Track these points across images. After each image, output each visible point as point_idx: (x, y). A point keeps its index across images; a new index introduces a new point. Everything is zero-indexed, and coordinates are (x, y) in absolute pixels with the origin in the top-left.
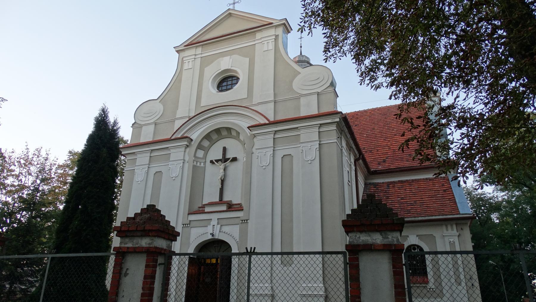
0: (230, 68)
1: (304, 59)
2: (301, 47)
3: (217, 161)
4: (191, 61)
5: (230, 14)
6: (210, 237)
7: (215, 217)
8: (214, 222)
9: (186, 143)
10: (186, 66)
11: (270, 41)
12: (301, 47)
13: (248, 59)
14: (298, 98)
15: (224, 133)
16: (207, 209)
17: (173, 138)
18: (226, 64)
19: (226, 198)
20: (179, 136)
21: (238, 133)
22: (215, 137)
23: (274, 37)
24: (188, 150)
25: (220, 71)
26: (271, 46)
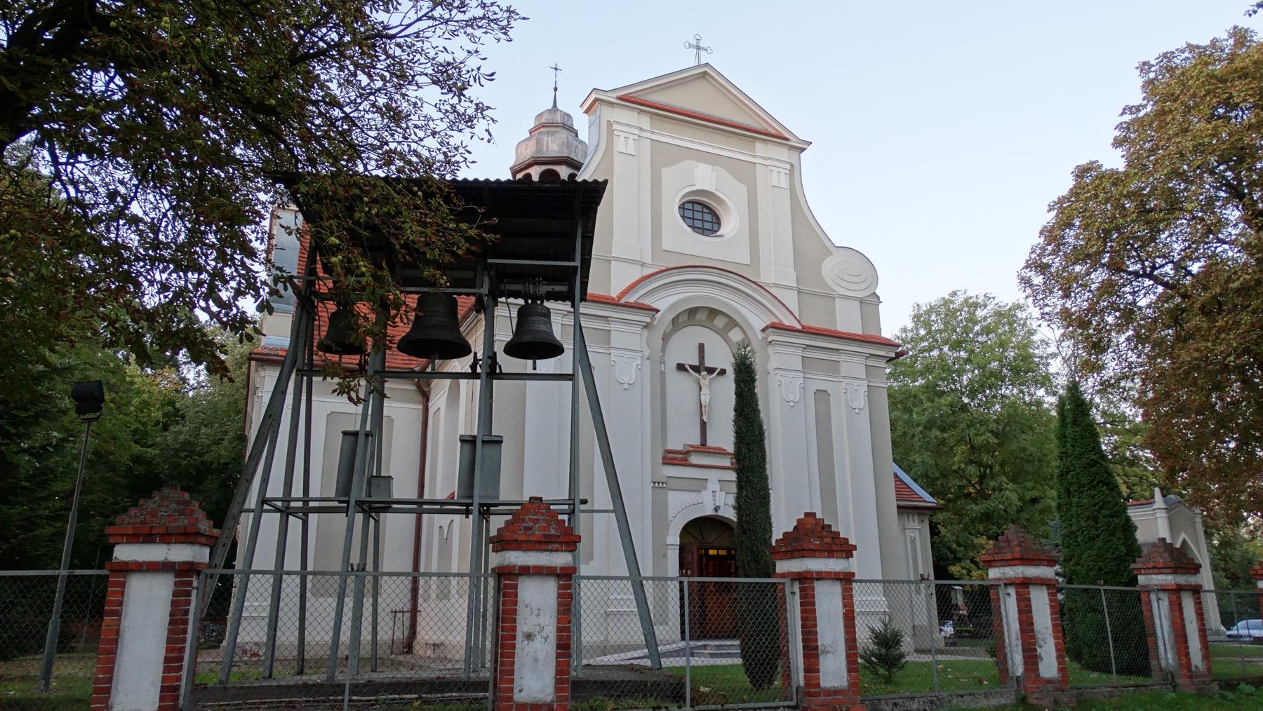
0: (713, 190)
1: (558, 118)
2: (556, 89)
3: (697, 369)
5: (705, 73)
6: (709, 512)
7: (713, 476)
8: (713, 485)
9: (648, 320)
10: (620, 145)
11: (783, 171)
12: (556, 89)
13: (744, 188)
14: (831, 298)
15: (701, 316)
16: (694, 459)
17: (622, 301)
18: (704, 178)
19: (711, 442)
20: (632, 299)
21: (732, 323)
22: (684, 318)
23: (788, 167)
24: (646, 333)
25: (695, 188)
26: (784, 183)
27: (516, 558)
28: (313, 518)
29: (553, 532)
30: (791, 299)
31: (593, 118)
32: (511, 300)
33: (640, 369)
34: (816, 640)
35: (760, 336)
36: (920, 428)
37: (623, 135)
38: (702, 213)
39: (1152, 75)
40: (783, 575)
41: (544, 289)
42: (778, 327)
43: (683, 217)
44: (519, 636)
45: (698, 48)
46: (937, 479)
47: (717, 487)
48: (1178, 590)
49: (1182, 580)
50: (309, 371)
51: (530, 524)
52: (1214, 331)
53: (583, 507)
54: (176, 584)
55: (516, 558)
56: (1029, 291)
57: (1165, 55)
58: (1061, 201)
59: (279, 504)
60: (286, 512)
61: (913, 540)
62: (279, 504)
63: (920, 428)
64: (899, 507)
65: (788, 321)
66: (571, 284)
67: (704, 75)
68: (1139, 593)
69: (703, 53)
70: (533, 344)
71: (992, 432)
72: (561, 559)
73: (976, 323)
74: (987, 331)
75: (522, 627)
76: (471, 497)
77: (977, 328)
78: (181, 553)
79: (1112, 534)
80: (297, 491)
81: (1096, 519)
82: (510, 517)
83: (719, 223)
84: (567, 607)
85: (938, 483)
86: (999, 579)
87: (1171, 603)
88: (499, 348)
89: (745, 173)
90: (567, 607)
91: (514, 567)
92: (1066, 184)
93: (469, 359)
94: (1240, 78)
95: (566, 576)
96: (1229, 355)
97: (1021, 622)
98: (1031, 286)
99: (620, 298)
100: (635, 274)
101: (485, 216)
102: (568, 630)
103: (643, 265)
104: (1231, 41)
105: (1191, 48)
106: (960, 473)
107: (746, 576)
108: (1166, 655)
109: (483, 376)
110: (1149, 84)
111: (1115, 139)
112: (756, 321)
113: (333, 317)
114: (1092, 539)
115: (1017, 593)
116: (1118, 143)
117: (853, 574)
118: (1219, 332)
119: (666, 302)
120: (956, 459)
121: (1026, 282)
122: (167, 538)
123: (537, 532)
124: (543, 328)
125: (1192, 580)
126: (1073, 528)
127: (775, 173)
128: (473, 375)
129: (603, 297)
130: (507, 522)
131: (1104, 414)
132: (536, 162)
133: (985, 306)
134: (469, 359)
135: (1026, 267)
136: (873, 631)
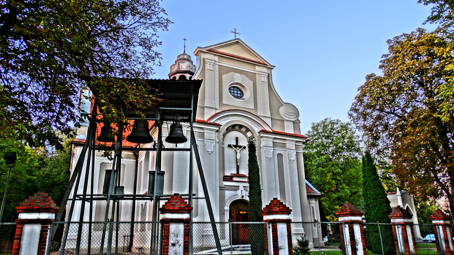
0: (241, 83)
1: (186, 57)
2: (185, 47)
4: (212, 64)
6: (240, 198)
7: (241, 185)
8: (241, 188)
9: (218, 129)
10: (207, 67)
11: (266, 76)
12: (185, 47)
13: (252, 82)
15: (237, 128)
16: (235, 179)
18: (238, 78)
20: (212, 121)
21: (248, 130)
24: (217, 133)
26: (266, 80)
27: (169, 216)
28: (95, 202)
29: (182, 206)
30: (269, 121)
31: (198, 57)
32: (168, 122)
33: (215, 146)
34: (278, 244)
35: (258, 134)
36: (315, 167)
37: (209, 63)
38: (237, 91)
39: (392, 44)
40: (266, 221)
41: (180, 118)
42: (264, 132)
43: (230, 92)
44: (170, 244)
45: (235, 33)
46: (321, 185)
47: (243, 189)
48: (404, 225)
49: (406, 220)
50: (93, 148)
51: (174, 203)
52: (415, 132)
53: (194, 197)
54: (42, 227)
55: (169, 216)
56: (352, 119)
57: (396, 37)
58: (362, 87)
59: (82, 197)
60: (84, 200)
61: (313, 208)
62: (82, 197)
63: (315, 167)
64: (307, 195)
65: (268, 129)
66: (189, 117)
67: (237, 42)
68: (391, 225)
69: (237, 35)
70: (176, 138)
71: (340, 168)
72: (185, 216)
73: (334, 130)
74: (338, 132)
75: (172, 240)
76: (153, 193)
77: (334, 131)
78: (44, 216)
79: (382, 205)
80: (89, 192)
81: (376, 199)
82: (167, 201)
83: (243, 94)
84: (188, 234)
85: (322, 186)
86: (343, 221)
87: (403, 229)
88: (163, 139)
89: (252, 77)
90: (188, 234)
91: (168, 219)
92: (363, 81)
93: (152, 143)
94: (421, 45)
95: (187, 223)
96: (421, 141)
97: (350, 237)
98: (352, 117)
99: (208, 121)
100: (213, 112)
101: (159, 92)
102: (188, 242)
103: (216, 109)
104: (418, 33)
105: (405, 35)
106: (329, 183)
107: (253, 221)
108: (401, 247)
109: (158, 150)
110: (391, 48)
111: (380, 66)
112: (257, 129)
113: (103, 129)
114: (375, 206)
115: (349, 226)
116: (381, 67)
117: (291, 220)
118: (417, 133)
119: (224, 123)
120: (328, 178)
121: (350, 115)
122: (39, 211)
123: (177, 207)
124: (180, 132)
125: (410, 221)
126: (369, 202)
127: (263, 77)
128: (154, 149)
129: (202, 121)
130: (166, 203)
131: (379, 161)
132: (178, 72)
133: (337, 124)
134: (152, 143)
135: (350, 110)
136: (298, 240)
